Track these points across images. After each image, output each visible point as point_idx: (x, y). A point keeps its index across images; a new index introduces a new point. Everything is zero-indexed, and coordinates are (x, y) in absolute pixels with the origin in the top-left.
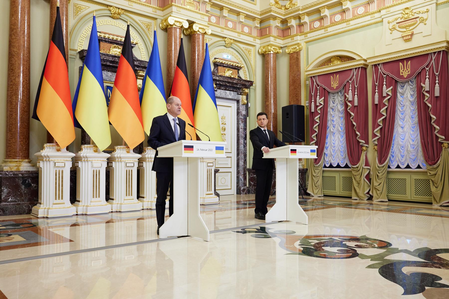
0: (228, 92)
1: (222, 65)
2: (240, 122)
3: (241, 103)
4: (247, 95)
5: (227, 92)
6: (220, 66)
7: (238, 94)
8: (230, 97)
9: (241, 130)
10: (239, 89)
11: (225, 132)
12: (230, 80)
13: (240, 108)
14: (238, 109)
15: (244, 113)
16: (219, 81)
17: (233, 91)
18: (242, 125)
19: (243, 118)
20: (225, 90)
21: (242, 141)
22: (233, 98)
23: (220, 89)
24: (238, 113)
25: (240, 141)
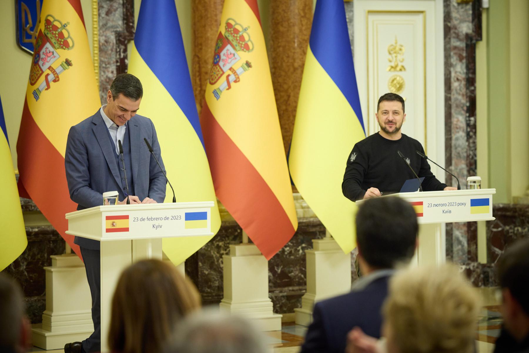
2: (454, 60)
9: (455, 85)
13: (454, 15)
14: (447, 17)
15: (466, 28)
18: (459, 69)
19: (462, 45)
21: (460, 119)
24: (448, 30)
25: (454, 120)
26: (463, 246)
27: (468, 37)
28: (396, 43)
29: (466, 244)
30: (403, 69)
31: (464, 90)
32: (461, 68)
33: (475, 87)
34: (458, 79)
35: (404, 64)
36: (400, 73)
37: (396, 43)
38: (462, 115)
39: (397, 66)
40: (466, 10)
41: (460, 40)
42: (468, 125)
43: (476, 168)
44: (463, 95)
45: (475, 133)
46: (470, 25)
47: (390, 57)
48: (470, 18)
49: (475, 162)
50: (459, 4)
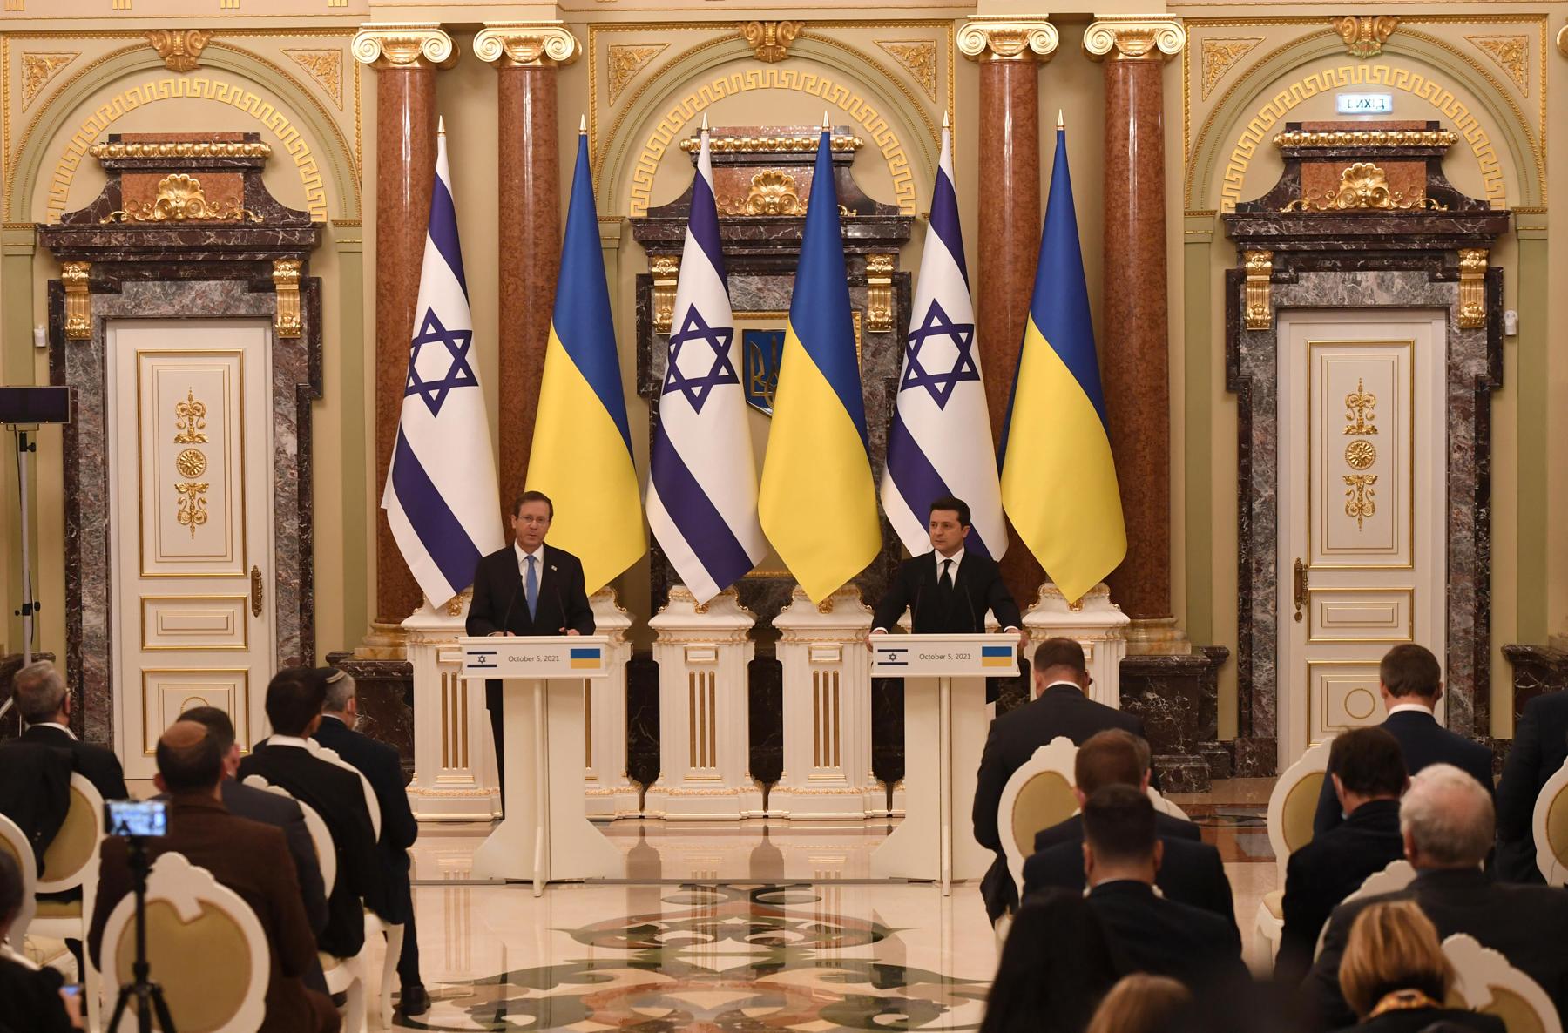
0: (1368, 279)
1: (1316, 154)
3: (1454, 322)
4: (1493, 280)
5: (1360, 276)
6: (1312, 159)
7: (1433, 279)
8: (1383, 299)
10: (1438, 254)
11: (1370, 473)
12: (1347, 228)
15: (1476, 367)
16: (1281, 238)
17: (1398, 268)
19: (1470, 394)
20: (1349, 267)
22: (1403, 302)
23: (1314, 269)
26: (1465, 710)
27: (1478, 381)
28: (1361, 390)
29: (1471, 708)
30: (1374, 430)
31: (1471, 465)
32: (1467, 430)
33: (1489, 461)
34: (1459, 448)
35: (1373, 423)
36: (1366, 437)
37: (1361, 390)
38: (1466, 503)
39: (1361, 426)
40: (1476, 339)
41: (1465, 387)
42: (1477, 520)
43: (1488, 588)
44: (1469, 473)
45: (1488, 533)
46: (1485, 362)
47: (1350, 412)
48: (1485, 352)
49: (1488, 578)
50: (1463, 330)
